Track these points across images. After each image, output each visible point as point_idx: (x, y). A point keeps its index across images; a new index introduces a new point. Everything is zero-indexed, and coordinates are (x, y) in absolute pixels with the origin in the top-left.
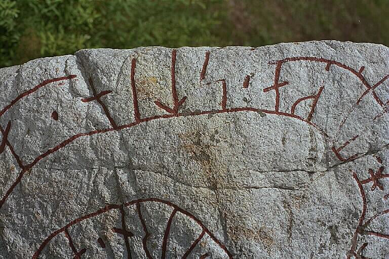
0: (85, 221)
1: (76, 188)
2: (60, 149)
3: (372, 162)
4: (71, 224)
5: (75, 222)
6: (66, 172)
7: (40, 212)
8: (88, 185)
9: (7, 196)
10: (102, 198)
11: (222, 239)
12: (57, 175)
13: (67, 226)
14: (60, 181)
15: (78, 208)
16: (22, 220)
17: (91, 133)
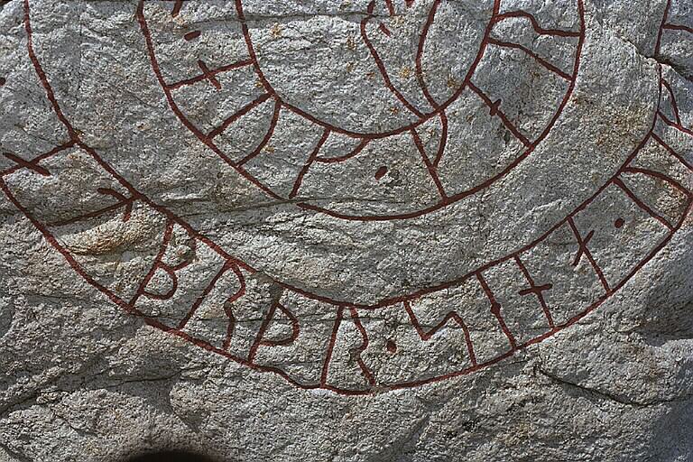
0: (158, 56)
1: (108, 63)
2: (49, 81)
4: (160, 78)
5: (157, 72)
6: (83, 76)
7: (138, 124)
8: (104, 44)
9: (113, 172)
10: (126, 25)
12: (87, 90)
13: (163, 83)
14: (96, 86)
15: (136, 66)
16: (149, 154)
17: (29, 31)
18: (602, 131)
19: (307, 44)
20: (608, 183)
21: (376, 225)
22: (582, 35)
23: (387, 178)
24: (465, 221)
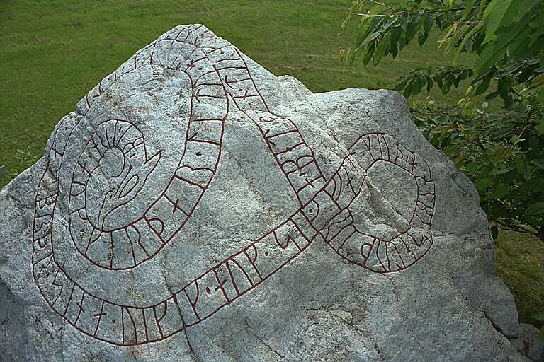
3: (188, 61)
11: (125, 119)
18: (130, 289)
20: (120, 305)
21: (71, 242)
24: (83, 266)
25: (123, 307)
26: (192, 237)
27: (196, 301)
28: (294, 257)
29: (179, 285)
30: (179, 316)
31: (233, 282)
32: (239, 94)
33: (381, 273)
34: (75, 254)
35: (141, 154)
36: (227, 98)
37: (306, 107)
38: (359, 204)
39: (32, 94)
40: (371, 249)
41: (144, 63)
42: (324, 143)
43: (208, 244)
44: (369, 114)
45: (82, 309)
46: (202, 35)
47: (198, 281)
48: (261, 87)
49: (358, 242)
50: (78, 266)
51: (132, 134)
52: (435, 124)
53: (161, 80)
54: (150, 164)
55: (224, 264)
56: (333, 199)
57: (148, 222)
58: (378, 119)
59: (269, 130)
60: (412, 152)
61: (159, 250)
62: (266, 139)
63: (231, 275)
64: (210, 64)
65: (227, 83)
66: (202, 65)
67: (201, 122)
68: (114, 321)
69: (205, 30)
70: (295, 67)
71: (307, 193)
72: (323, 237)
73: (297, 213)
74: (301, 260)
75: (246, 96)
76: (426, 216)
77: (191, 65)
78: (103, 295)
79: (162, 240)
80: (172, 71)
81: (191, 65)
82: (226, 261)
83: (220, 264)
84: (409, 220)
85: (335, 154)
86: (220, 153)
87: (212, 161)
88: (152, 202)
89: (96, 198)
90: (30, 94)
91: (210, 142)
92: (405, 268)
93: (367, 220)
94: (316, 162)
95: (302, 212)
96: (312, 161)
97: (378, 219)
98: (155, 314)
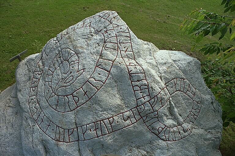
3: (105, 29)
19: (58, 74)
21: (43, 93)
22: (71, 111)
23: (48, 92)
25: (57, 126)
26: (89, 108)
27: (85, 133)
28: (128, 126)
29: (80, 124)
30: (77, 136)
31: (101, 130)
32: (124, 49)
33: (164, 140)
34: (44, 99)
35: (76, 68)
36: (118, 50)
37: (152, 61)
38: (164, 110)
39: (47, 10)
40: (163, 130)
41: (87, 26)
42: (155, 81)
43: (95, 112)
44: (181, 68)
45: (42, 121)
46: (114, 18)
47: (87, 125)
48: (134, 48)
49: (159, 126)
50: (44, 104)
51: (75, 58)
52: (213, 73)
53: (92, 35)
54: (79, 73)
55: (99, 122)
56: (151, 106)
57: (73, 97)
58: (184, 72)
59: (131, 71)
60: (196, 89)
61: (75, 109)
62: (130, 74)
63: (101, 127)
64: (114, 33)
65: (119, 43)
66: (111, 33)
67: (104, 60)
68: (53, 130)
69: (116, 15)
70: (161, 20)
71: (141, 101)
72: (143, 120)
73: (135, 108)
74: (131, 127)
75: (126, 51)
76: (193, 119)
77: (106, 32)
78: (51, 119)
79: (77, 105)
80: (97, 32)
81: (106, 32)
82: (100, 121)
83: (97, 122)
84: (184, 120)
85: (159, 86)
86: (108, 76)
87: (104, 78)
88: (76, 89)
89: (56, 80)
90: (46, 10)
91: (106, 70)
92: (175, 141)
93: (165, 118)
94: (148, 89)
95: (137, 108)
96: (147, 88)
97: (170, 117)
98: (68, 132)
